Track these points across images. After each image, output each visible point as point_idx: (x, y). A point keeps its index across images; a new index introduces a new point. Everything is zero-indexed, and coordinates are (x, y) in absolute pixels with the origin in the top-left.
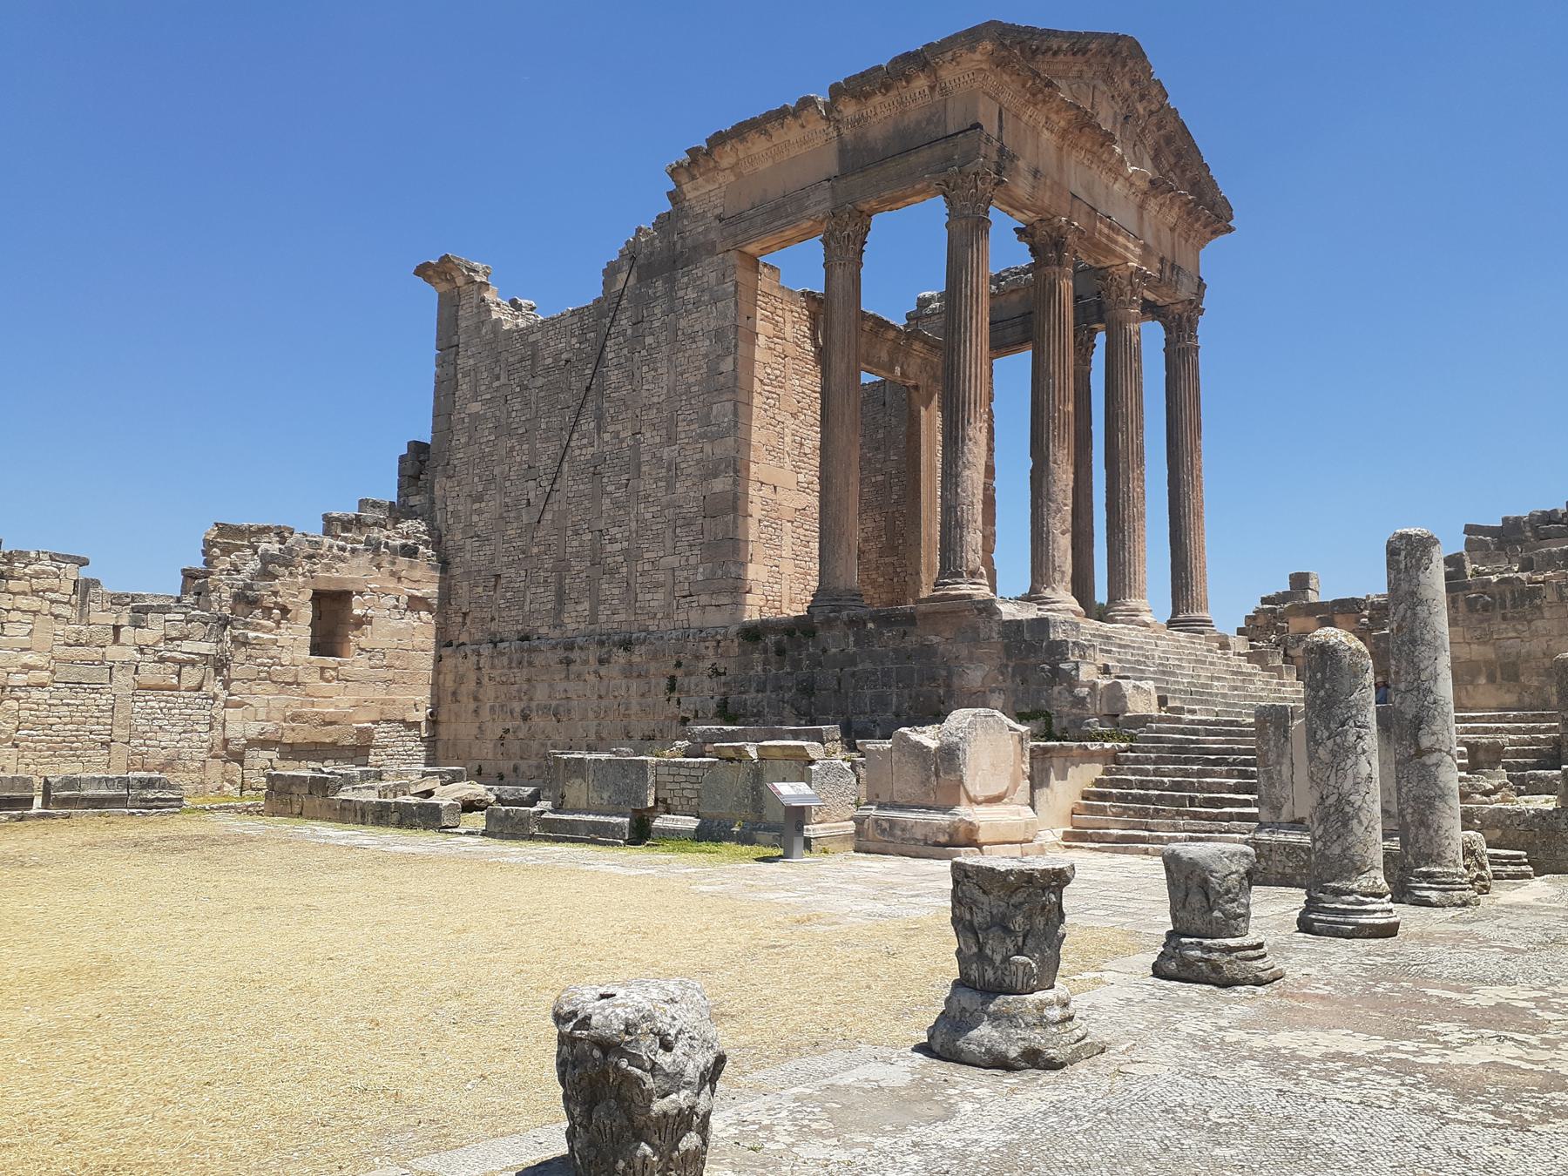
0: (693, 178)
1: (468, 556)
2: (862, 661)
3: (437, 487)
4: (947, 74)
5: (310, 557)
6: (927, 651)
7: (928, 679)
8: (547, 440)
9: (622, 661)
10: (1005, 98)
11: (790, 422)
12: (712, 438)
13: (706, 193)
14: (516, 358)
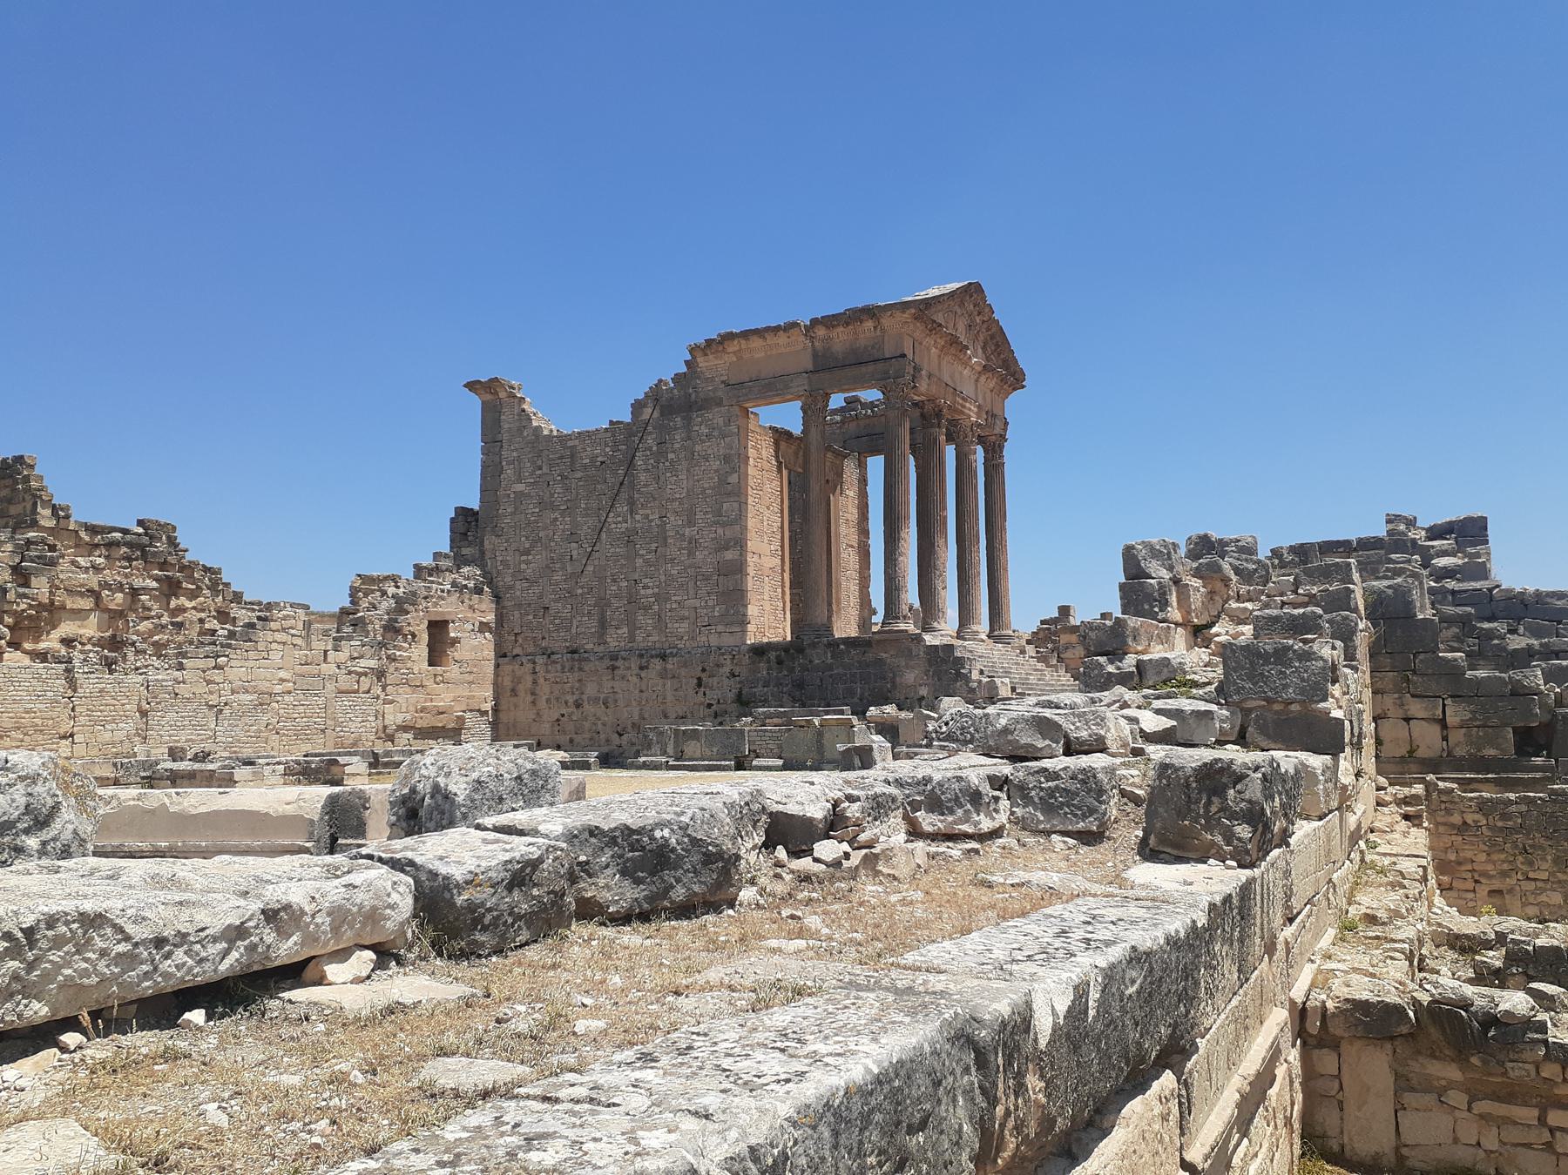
0: (706, 355)
1: (518, 593)
2: (837, 668)
3: (486, 542)
4: (886, 321)
5: (426, 598)
6: (880, 662)
7: (881, 678)
8: (587, 515)
9: (658, 667)
10: (917, 334)
11: (766, 512)
12: (724, 525)
13: (715, 366)
14: (557, 456)
